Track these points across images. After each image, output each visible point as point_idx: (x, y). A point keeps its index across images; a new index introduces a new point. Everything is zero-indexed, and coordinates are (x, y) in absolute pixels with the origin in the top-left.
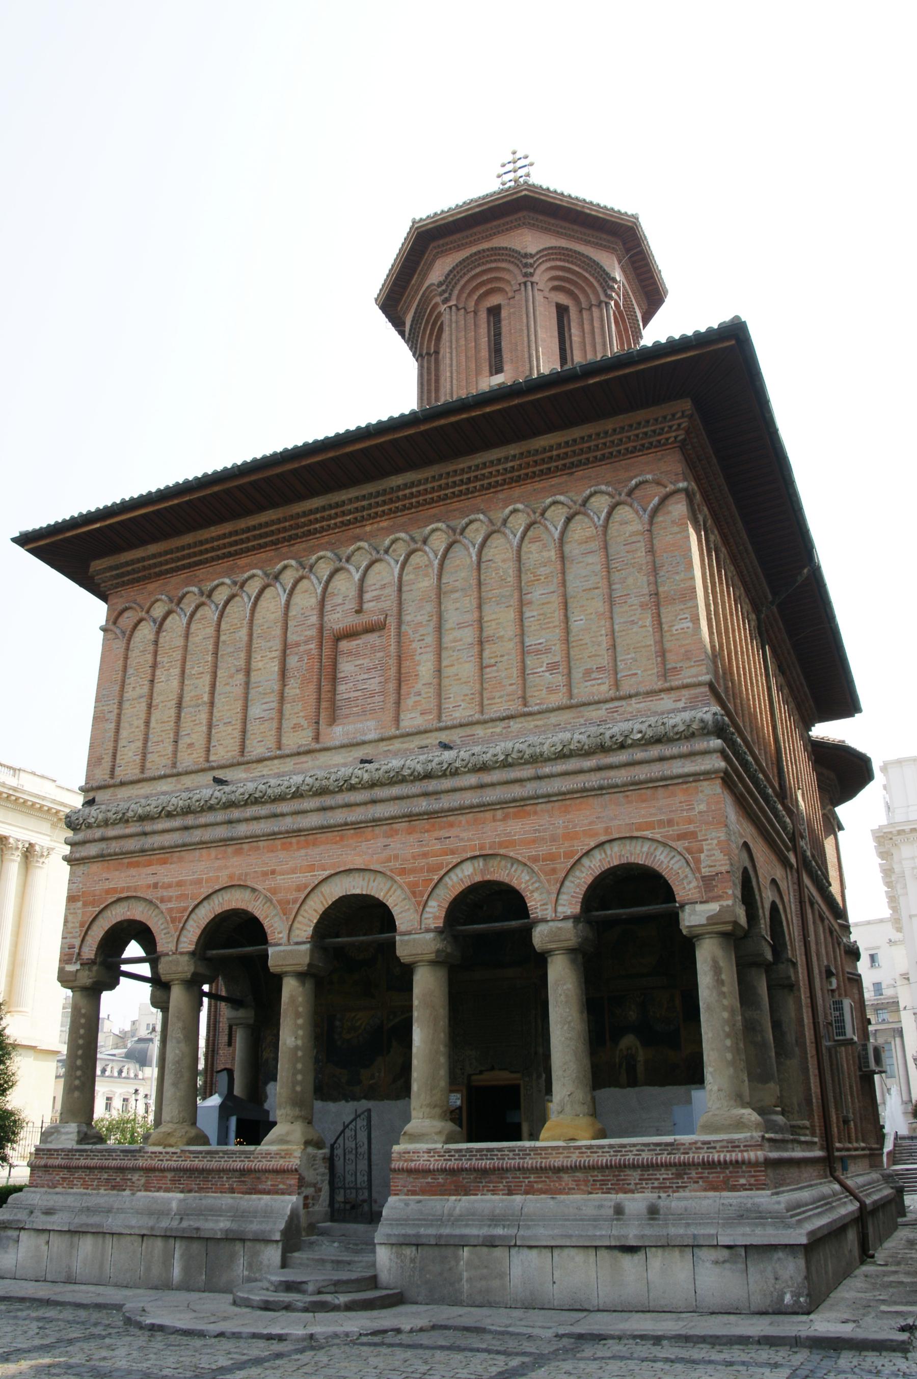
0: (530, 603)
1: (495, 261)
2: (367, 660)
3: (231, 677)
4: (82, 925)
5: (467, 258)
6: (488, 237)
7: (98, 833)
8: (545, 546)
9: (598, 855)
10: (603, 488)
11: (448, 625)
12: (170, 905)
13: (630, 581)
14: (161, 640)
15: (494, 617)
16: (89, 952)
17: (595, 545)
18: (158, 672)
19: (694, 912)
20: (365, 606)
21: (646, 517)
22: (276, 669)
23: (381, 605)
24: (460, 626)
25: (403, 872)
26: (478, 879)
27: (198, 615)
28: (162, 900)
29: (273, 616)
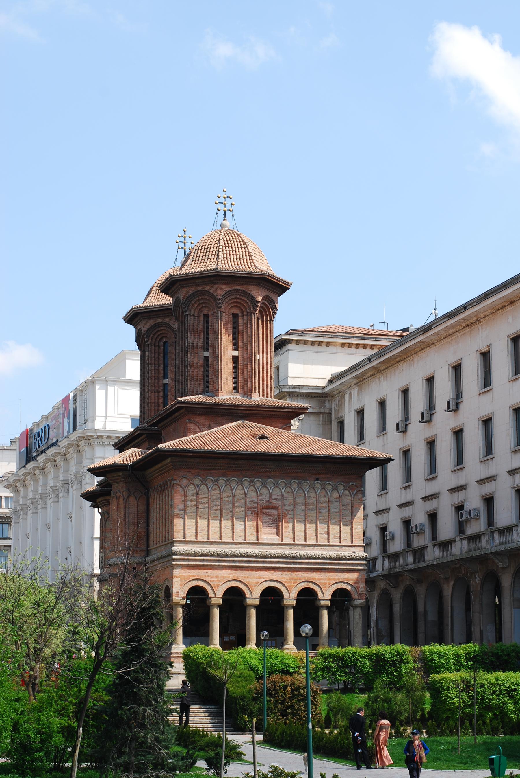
0: (320, 513)
1: (242, 296)
2: (272, 518)
3: (228, 513)
4: (181, 586)
5: (232, 290)
6: (242, 285)
7: (186, 557)
8: (325, 496)
9: (336, 585)
10: (342, 483)
11: (298, 513)
12: (213, 583)
13: (347, 513)
14: (200, 493)
15: (311, 514)
16: (184, 594)
17: (338, 500)
18: (200, 505)
19: (357, 601)
20: (273, 501)
21: (353, 496)
22: (244, 514)
23: (277, 502)
24: (301, 514)
25: (286, 582)
26: (306, 587)
27: (214, 488)
28: (211, 581)
29: (242, 496)
